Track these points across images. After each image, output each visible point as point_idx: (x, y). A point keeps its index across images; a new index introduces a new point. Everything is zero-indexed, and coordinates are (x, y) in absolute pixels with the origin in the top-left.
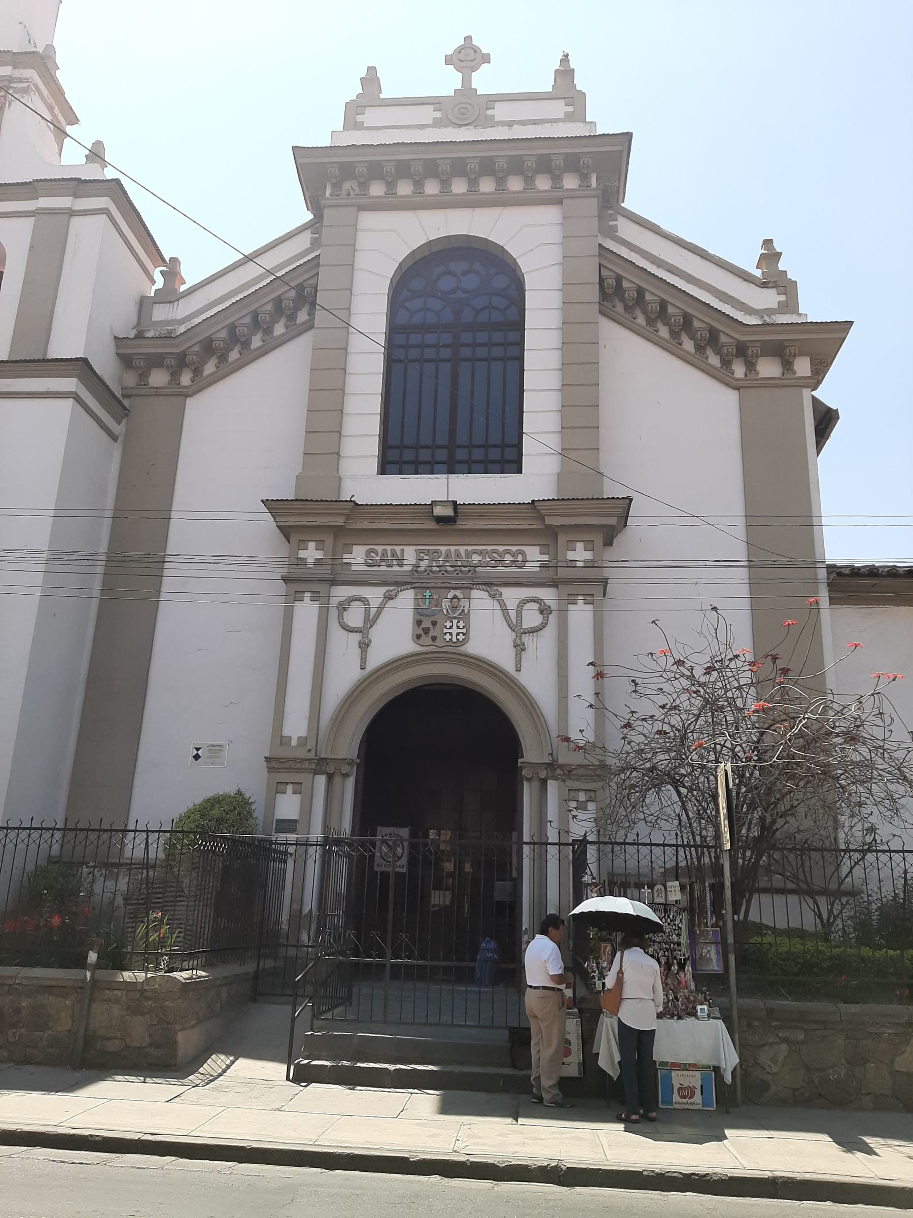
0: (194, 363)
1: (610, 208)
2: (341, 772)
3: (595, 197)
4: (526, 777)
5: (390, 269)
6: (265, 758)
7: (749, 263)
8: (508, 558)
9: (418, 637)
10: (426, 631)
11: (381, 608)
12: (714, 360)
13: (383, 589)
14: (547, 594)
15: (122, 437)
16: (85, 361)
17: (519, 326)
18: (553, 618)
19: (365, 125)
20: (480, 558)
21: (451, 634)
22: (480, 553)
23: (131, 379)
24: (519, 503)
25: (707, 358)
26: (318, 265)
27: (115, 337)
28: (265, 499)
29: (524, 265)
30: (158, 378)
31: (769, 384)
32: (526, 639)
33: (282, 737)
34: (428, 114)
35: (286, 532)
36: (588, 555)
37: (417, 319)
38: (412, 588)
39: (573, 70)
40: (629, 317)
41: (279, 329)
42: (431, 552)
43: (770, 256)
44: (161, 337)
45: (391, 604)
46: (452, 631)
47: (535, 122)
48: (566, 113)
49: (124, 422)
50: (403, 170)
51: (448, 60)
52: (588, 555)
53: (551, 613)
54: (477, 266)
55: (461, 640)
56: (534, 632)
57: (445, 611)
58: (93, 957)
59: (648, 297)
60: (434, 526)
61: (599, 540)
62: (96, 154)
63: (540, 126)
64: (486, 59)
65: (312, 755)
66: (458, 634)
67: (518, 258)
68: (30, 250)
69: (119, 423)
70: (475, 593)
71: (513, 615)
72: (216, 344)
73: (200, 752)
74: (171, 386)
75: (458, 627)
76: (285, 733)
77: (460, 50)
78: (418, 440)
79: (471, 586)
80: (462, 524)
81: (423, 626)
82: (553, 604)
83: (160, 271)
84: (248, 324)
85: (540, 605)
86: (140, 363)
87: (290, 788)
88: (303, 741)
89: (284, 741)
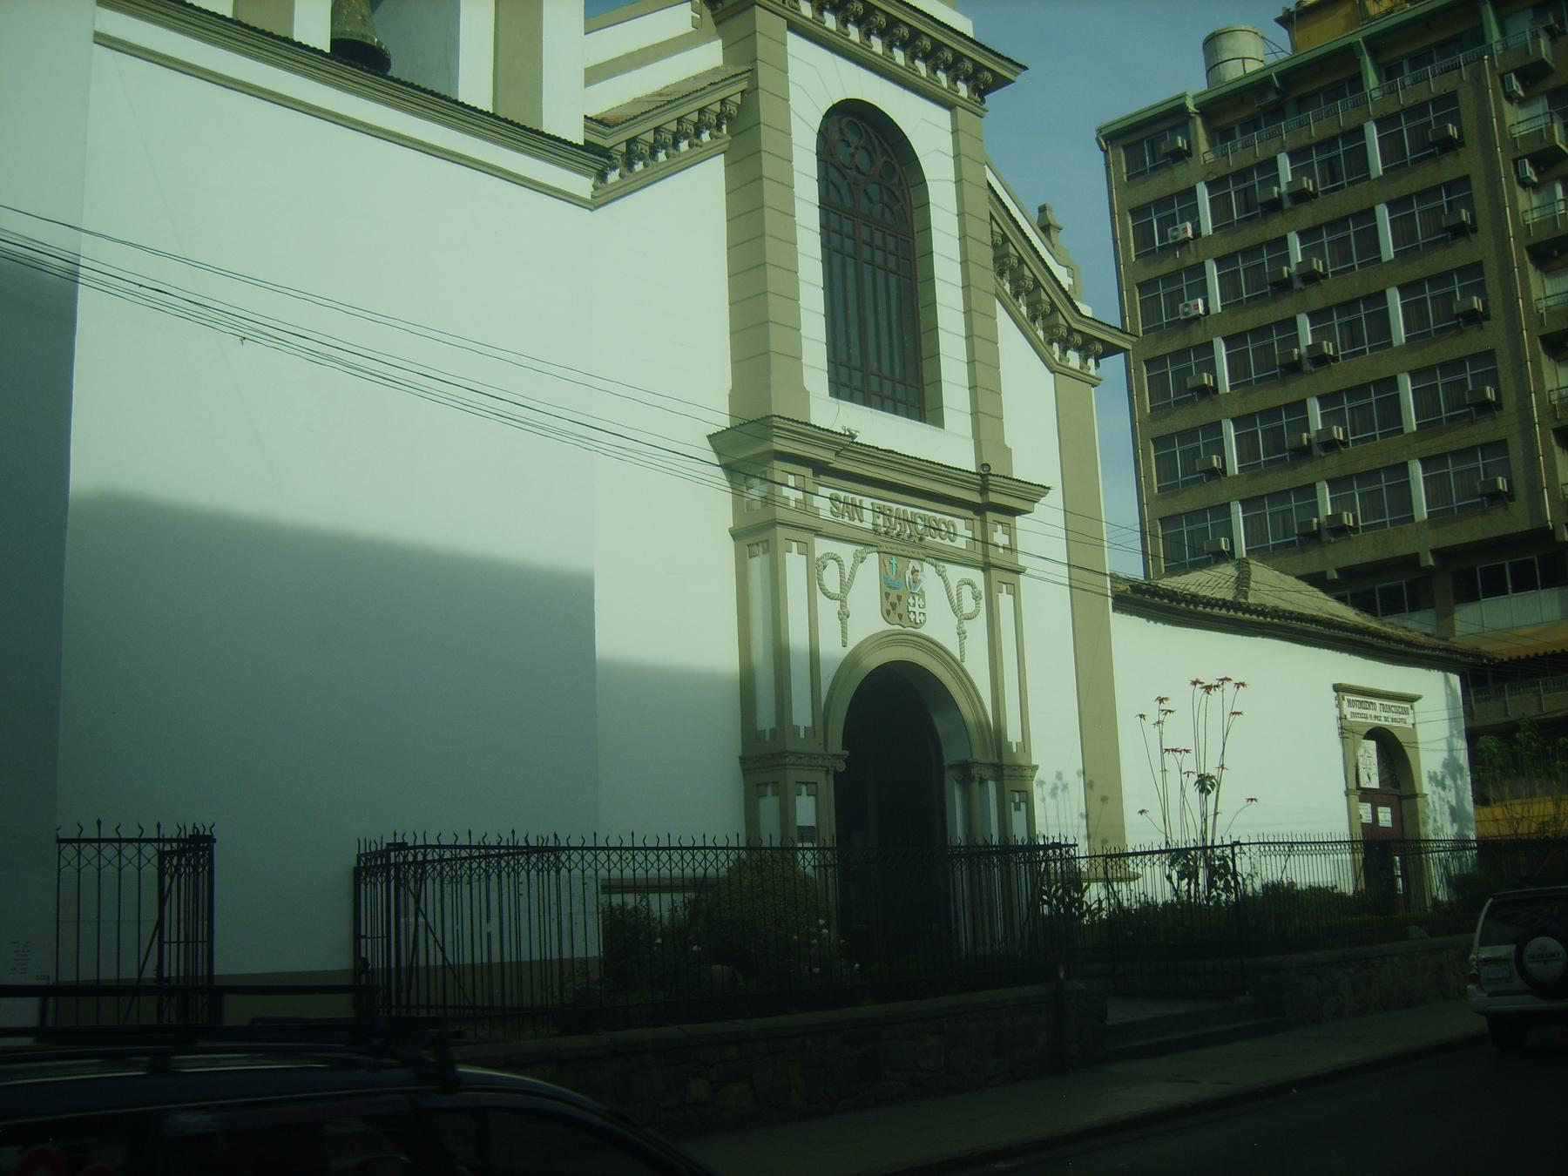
2: (836, 772)
5: (816, 121)
9: (888, 613)
10: (893, 606)
11: (854, 568)
13: (854, 548)
14: (977, 576)
21: (914, 612)
22: (923, 518)
32: (967, 625)
52: (1007, 542)
65: (821, 750)
66: (920, 613)
76: (795, 722)
79: (922, 557)
85: (973, 588)
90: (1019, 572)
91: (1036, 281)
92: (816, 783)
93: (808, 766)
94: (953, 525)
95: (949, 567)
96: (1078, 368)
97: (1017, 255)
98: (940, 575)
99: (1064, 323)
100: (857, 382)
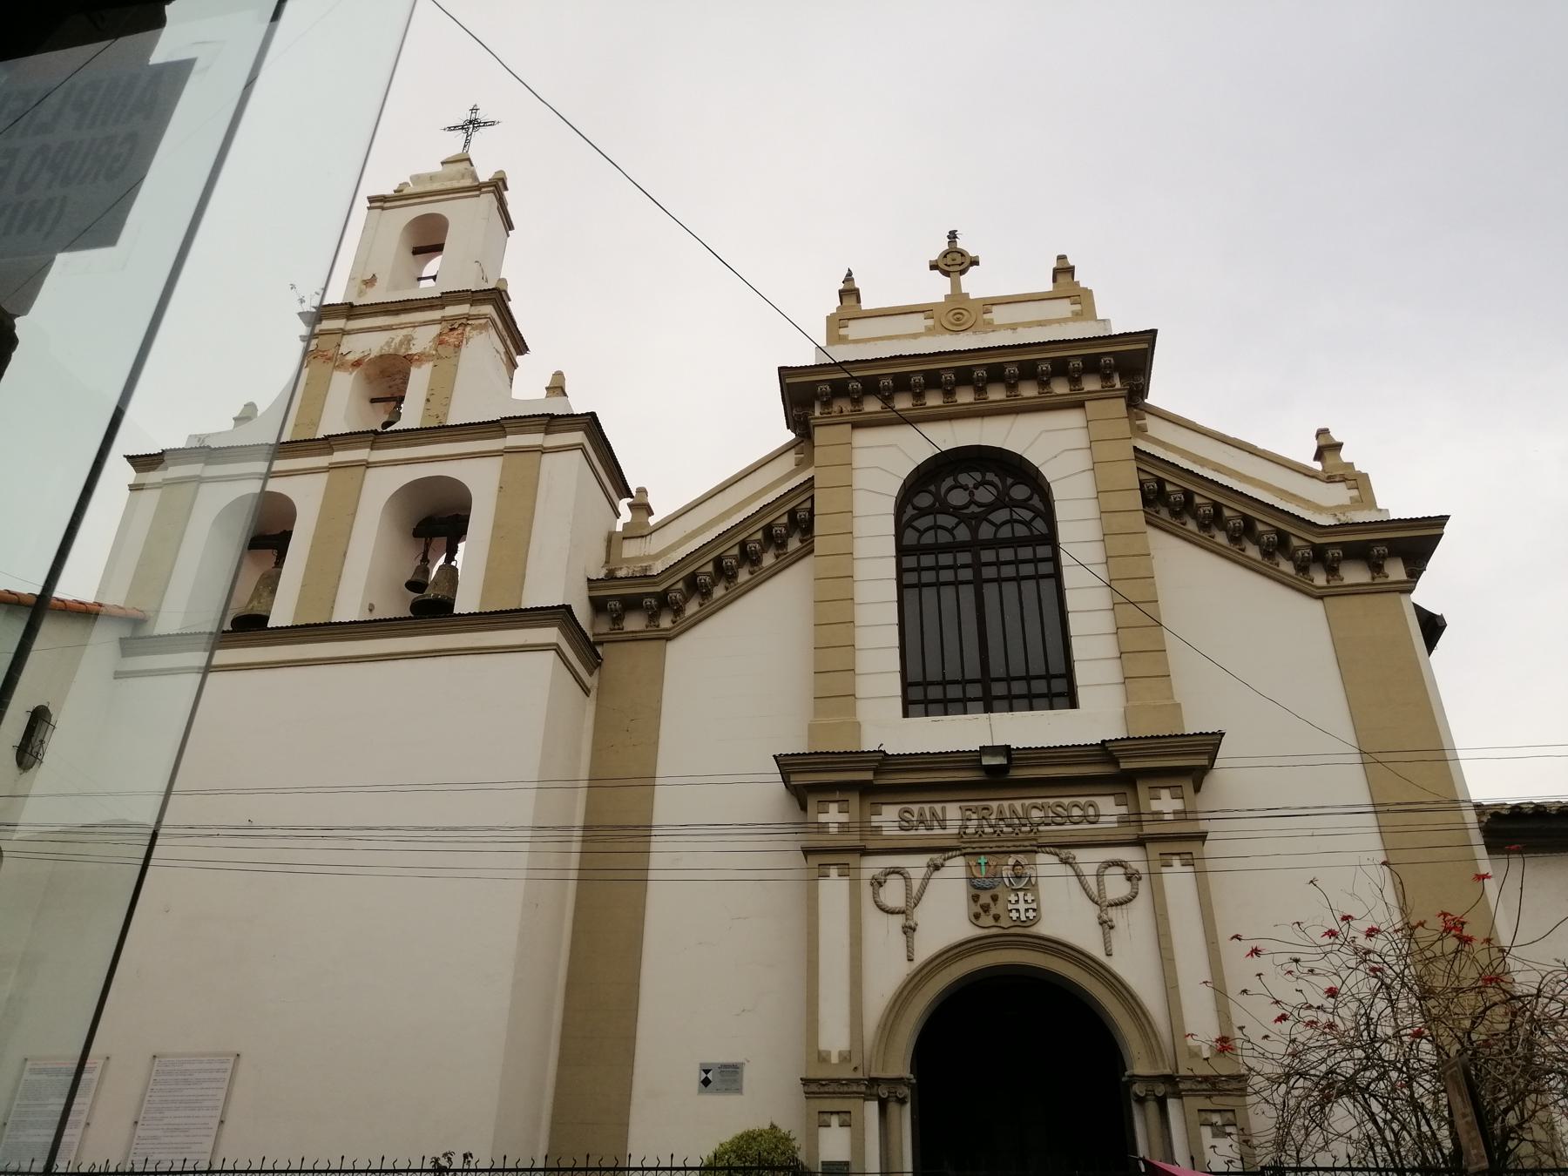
0: (677, 603)
1: (1135, 407)
2: (897, 1097)
3: (1121, 397)
4: (1136, 1095)
5: (894, 487)
6: (801, 1079)
8: (1076, 812)
9: (977, 916)
10: (986, 908)
11: (926, 879)
12: (1287, 567)
13: (923, 860)
15: (595, 690)
16: (568, 608)
17: (1050, 538)
18: (1143, 886)
19: (850, 338)
20: (1042, 814)
21: (1018, 910)
23: (604, 627)
24: (1086, 745)
25: (1278, 565)
26: (812, 487)
27: (588, 579)
28: (777, 754)
29: (1048, 472)
32: (1113, 913)
33: (819, 1053)
34: (918, 323)
35: (801, 795)
36: (1178, 805)
37: (928, 538)
38: (961, 855)
39: (1073, 267)
40: (1175, 523)
41: (768, 559)
42: (980, 809)
43: (1327, 448)
44: (636, 577)
45: (936, 874)
46: (1017, 906)
47: (1041, 324)
48: (1073, 312)
49: (596, 672)
50: (902, 383)
51: (934, 267)
52: (1178, 805)
53: (1140, 879)
54: (990, 476)
55: (1031, 918)
56: (1121, 904)
57: (1006, 881)
59: (1198, 500)
61: (1188, 786)
62: (557, 388)
63: (1048, 327)
64: (975, 262)
65: (859, 1075)
66: (1027, 910)
67: (1041, 465)
68: (500, 491)
69: (591, 674)
70: (1041, 858)
71: (1092, 882)
72: (702, 579)
73: (710, 1076)
74: (649, 629)
75: (1026, 901)
76: (823, 1046)
77: (945, 255)
78: (944, 674)
79: (1035, 848)
81: (982, 901)
82: (1141, 867)
83: (630, 506)
84: (736, 555)
85: (1126, 868)
86: (615, 605)
87: (835, 1120)
88: (845, 1058)
89: (823, 1058)
90: (1202, 837)
91: (1245, 517)
92: (850, 1112)
93: (834, 1093)
94: (1092, 806)
95: (1081, 855)
96: (1325, 583)
97: (1207, 501)
98: (1065, 863)
99: (1304, 543)
100: (975, 690)
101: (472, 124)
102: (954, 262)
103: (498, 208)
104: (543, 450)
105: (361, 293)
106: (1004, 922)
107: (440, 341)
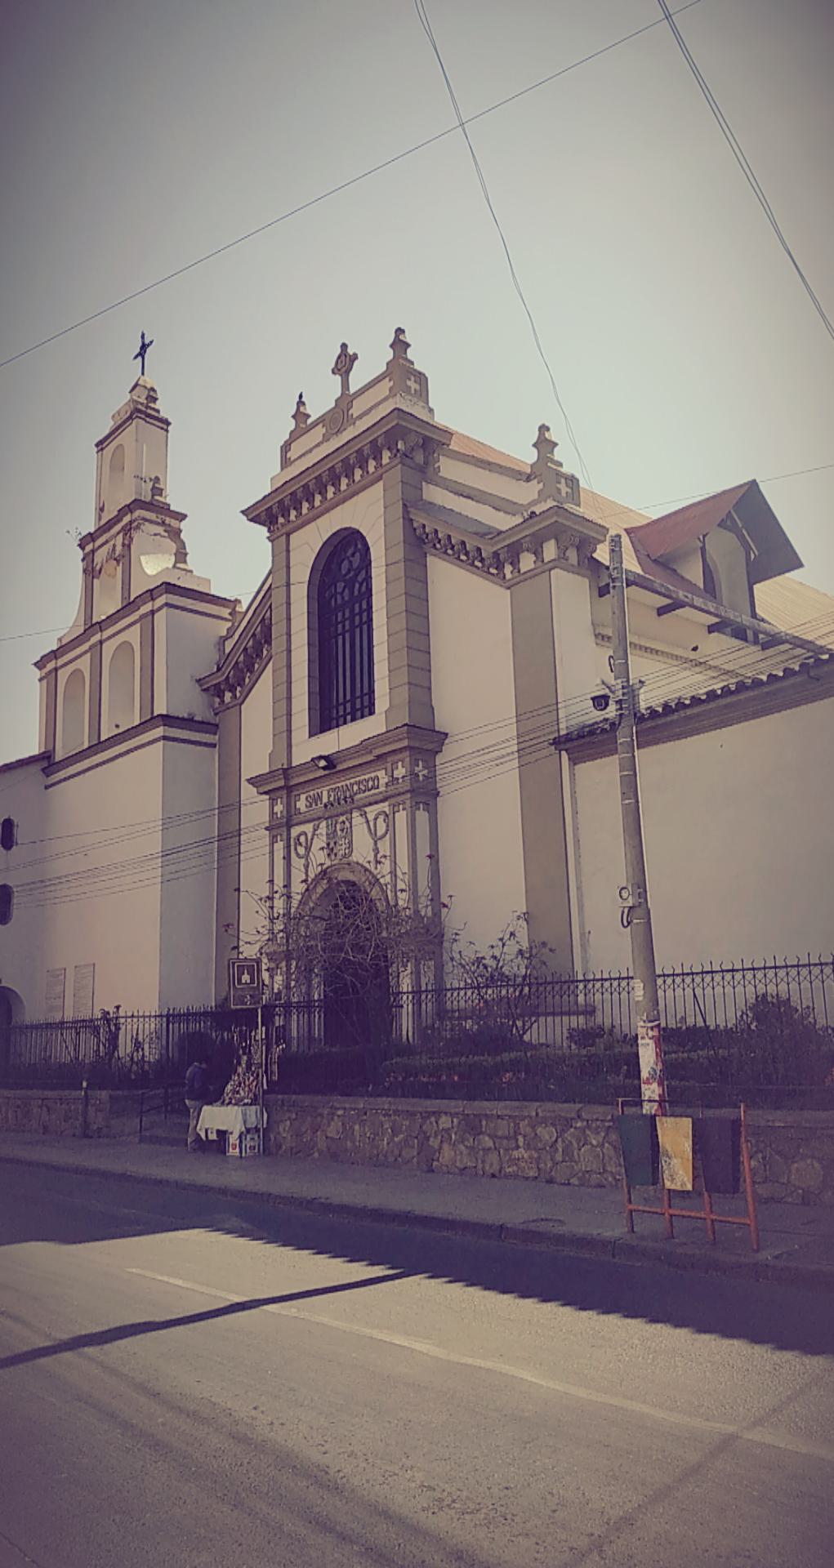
1: (434, 453)
7: (529, 456)
8: (371, 783)
9: (329, 855)
11: (312, 839)
13: (312, 824)
22: (358, 783)
23: (217, 700)
30: (228, 696)
31: (532, 574)
34: (320, 430)
46: (341, 850)
49: (218, 733)
58: (85, 1084)
60: (327, 772)
69: (215, 734)
80: (340, 767)
81: (331, 847)
101: (144, 347)
102: (345, 363)
103: (146, 421)
104: (153, 612)
105: (100, 519)
106: (339, 857)
107: (123, 545)
